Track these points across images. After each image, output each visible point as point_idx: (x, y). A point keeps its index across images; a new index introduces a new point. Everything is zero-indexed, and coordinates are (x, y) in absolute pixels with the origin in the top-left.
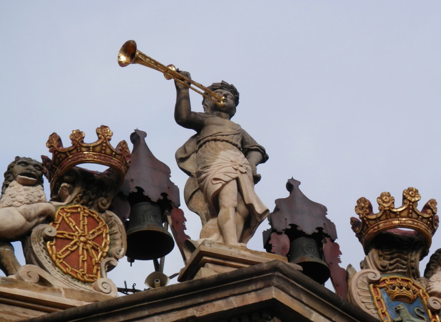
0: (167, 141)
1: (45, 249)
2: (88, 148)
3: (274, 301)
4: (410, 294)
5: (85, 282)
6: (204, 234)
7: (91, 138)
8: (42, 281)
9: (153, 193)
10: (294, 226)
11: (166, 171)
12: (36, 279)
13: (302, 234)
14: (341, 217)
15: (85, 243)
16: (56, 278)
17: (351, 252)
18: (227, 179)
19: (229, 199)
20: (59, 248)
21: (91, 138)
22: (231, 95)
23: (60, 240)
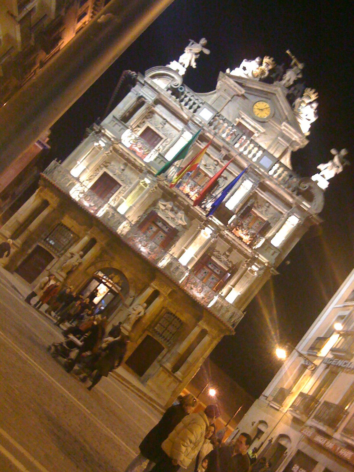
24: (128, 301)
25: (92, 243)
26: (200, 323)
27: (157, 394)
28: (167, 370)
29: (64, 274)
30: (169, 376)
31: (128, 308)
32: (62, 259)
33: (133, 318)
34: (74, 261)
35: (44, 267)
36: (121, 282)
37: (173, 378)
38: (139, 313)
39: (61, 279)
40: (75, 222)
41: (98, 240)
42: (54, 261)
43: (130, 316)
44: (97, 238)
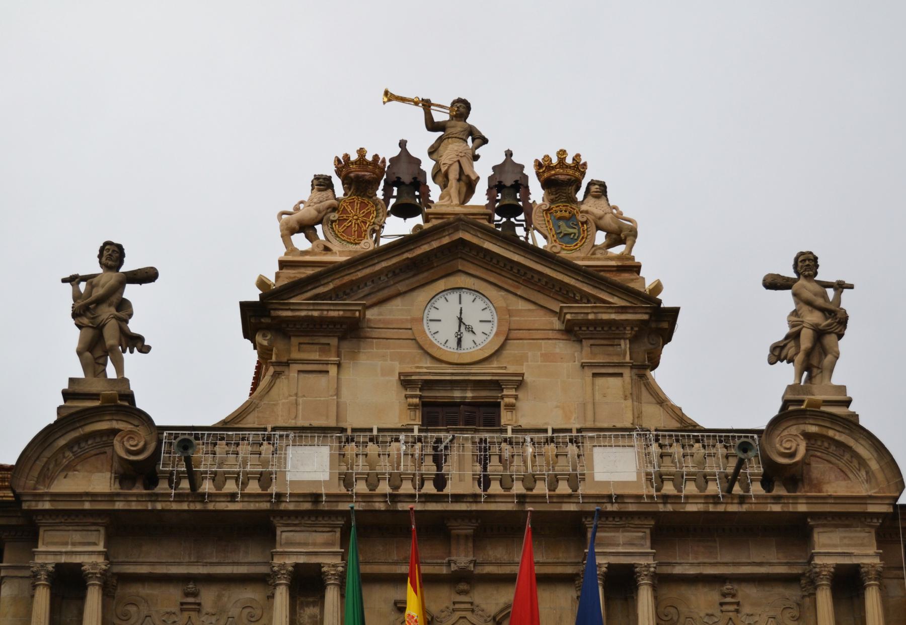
1: (332, 228)
2: (352, 163)
3: (461, 239)
4: (567, 214)
5: (356, 244)
6: (441, 198)
7: (354, 157)
8: (327, 249)
9: (407, 179)
10: (500, 182)
11: (418, 162)
12: (322, 247)
13: (505, 186)
14: (530, 171)
15: (357, 220)
16: (336, 246)
17: (537, 193)
18: (450, 162)
19: (453, 175)
20: (339, 225)
21: (354, 157)
22: (107, 247)
23: (340, 221)
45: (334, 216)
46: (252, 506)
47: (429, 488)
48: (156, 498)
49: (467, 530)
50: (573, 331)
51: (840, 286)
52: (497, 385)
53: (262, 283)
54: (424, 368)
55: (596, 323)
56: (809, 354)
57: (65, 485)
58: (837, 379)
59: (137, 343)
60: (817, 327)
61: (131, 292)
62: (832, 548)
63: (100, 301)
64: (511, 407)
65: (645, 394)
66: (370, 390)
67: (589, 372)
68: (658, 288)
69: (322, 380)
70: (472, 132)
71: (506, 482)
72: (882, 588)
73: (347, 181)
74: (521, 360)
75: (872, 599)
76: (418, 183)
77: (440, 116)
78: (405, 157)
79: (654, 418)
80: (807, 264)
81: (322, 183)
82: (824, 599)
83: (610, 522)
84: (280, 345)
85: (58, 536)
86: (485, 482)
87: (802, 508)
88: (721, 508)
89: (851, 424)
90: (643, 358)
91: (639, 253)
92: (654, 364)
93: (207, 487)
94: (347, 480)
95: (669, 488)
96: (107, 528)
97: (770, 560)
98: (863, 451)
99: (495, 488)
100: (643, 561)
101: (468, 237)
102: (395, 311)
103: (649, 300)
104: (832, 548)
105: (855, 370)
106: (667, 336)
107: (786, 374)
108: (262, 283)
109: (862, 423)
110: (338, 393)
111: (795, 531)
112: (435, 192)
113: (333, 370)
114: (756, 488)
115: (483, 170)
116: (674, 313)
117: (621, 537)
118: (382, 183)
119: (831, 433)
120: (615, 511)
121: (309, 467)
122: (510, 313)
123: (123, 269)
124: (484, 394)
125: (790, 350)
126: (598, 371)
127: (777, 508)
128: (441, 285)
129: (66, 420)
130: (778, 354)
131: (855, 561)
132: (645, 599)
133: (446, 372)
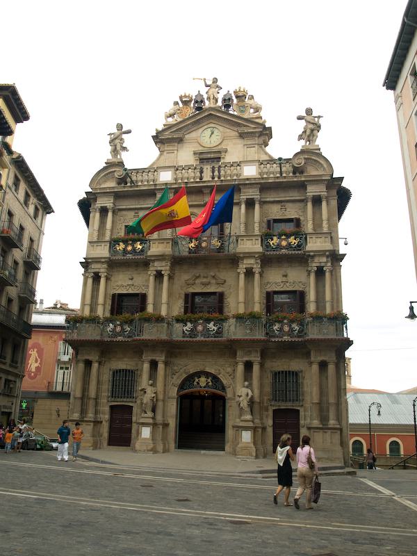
0: (204, 91)
9: (199, 100)
17: (235, 101)
24: (229, 394)
25: (154, 365)
26: (312, 359)
27: (328, 459)
28: (317, 428)
29: (150, 414)
30: (326, 432)
31: (234, 399)
32: (139, 402)
33: (244, 404)
34: (150, 393)
35: (131, 422)
36: (209, 380)
37: (330, 431)
38: (247, 395)
39: (151, 421)
40: (125, 359)
41: (157, 359)
42: (135, 410)
43: (241, 405)
44: (154, 358)
45: (179, 112)
46: (150, 188)
47: (198, 180)
48: (124, 187)
49: (206, 191)
50: (242, 136)
51: (319, 117)
52: (220, 152)
53: (157, 130)
54: (200, 149)
55: (248, 133)
56: (309, 136)
57: (103, 186)
58: (316, 143)
59: (124, 149)
60: (312, 128)
61: (124, 136)
62: (312, 190)
63: (115, 139)
64: (224, 158)
65: (262, 152)
66: (185, 155)
67: (246, 147)
68: (265, 121)
69: (173, 154)
70: (217, 87)
71: (219, 178)
72: (327, 202)
73: (182, 102)
74: (227, 145)
75: (324, 204)
76: (202, 101)
77: (209, 83)
78: (199, 95)
79: (265, 158)
80: (309, 112)
81: (176, 103)
82: (310, 205)
83: (247, 186)
84: (163, 146)
85: (101, 199)
86: (213, 178)
87: (303, 179)
88: (279, 180)
89: (320, 155)
90: (261, 142)
91: (262, 114)
92: (266, 145)
93: (140, 184)
94: (176, 179)
95: (265, 176)
96: (114, 196)
97: (295, 195)
98: (322, 162)
99: (216, 179)
100: (256, 197)
101: (212, 113)
102: (193, 135)
103: (263, 125)
104: (312, 190)
105: (323, 142)
106: (270, 136)
107: (303, 142)
108: (157, 130)
109: (323, 154)
110: (177, 158)
111: (302, 186)
112: (207, 103)
113: (176, 152)
114: (291, 174)
115: (220, 97)
116: (270, 128)
117: (251, 190)
118: (193, 102)
119: (313, 157)
120: (248, 183)
121: (166, 177)
122: (224, 133)
123: (123, 130)
124: (216, 155)
125: (303, 136)
126: (249, 146)
127: (295, 180)
128: (206, 127)
129: (105, 169)
130: (300, 137)
131: (319, 194)
132: (257, 206)
133: (205, 150)
